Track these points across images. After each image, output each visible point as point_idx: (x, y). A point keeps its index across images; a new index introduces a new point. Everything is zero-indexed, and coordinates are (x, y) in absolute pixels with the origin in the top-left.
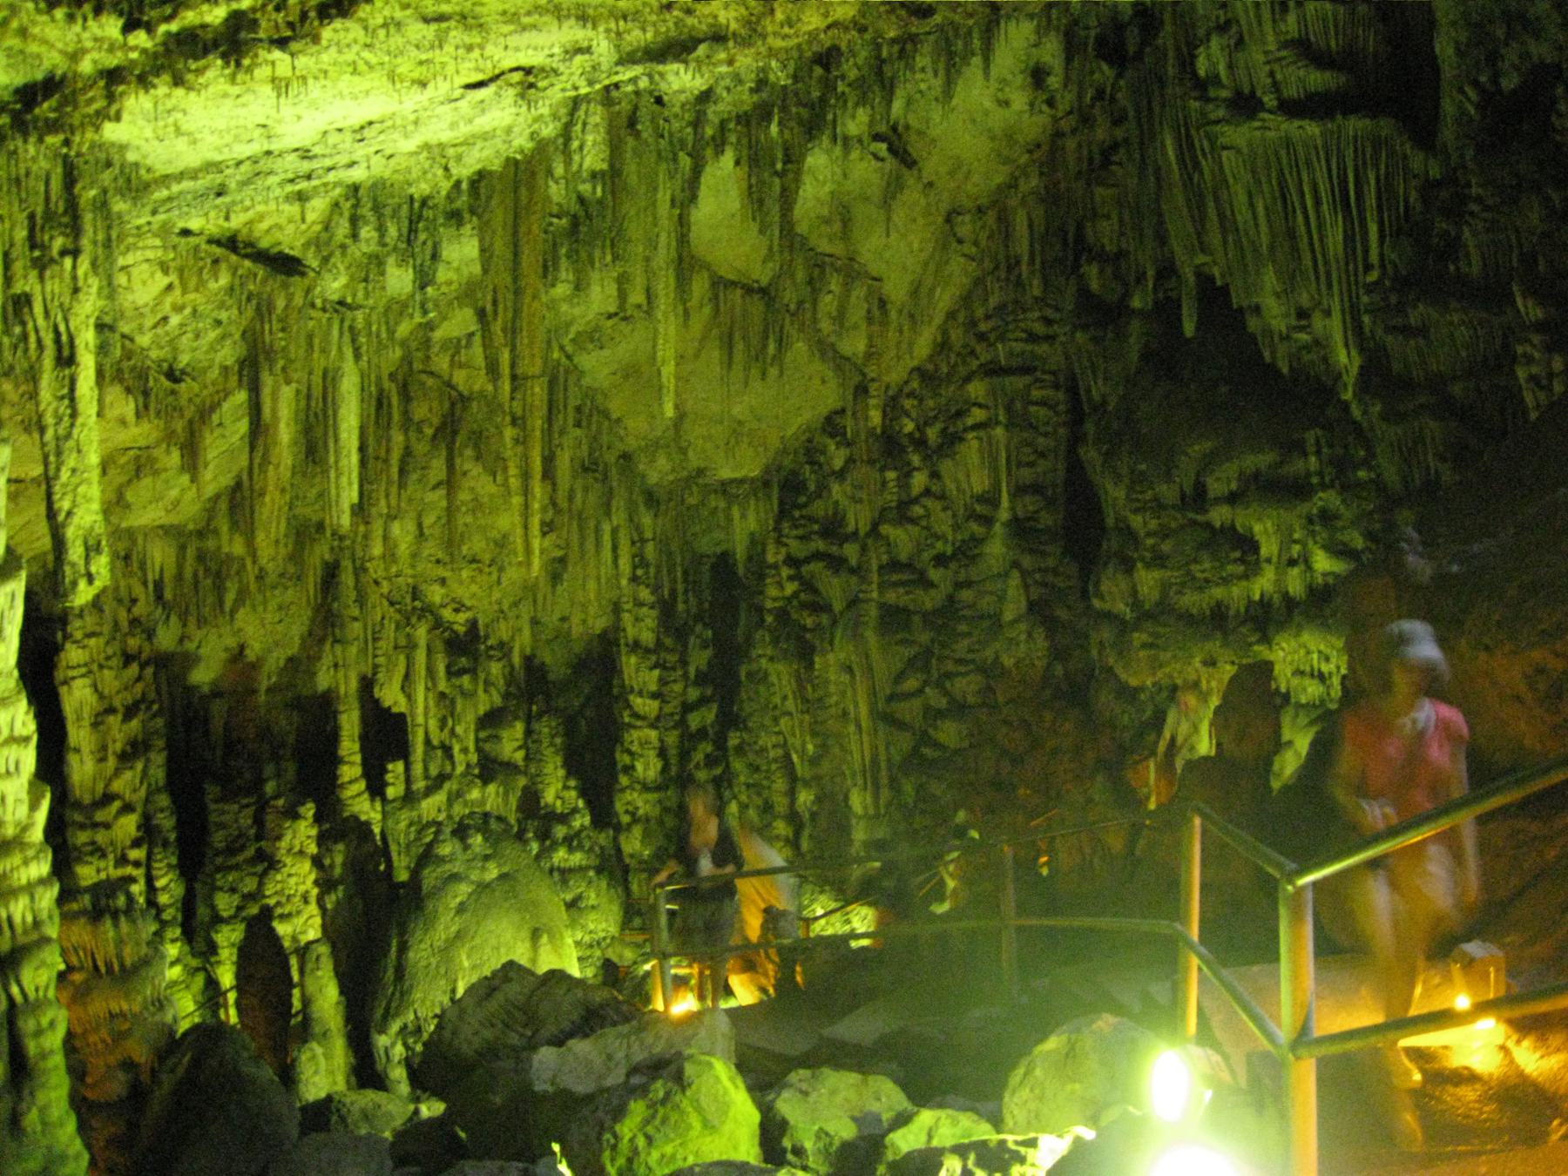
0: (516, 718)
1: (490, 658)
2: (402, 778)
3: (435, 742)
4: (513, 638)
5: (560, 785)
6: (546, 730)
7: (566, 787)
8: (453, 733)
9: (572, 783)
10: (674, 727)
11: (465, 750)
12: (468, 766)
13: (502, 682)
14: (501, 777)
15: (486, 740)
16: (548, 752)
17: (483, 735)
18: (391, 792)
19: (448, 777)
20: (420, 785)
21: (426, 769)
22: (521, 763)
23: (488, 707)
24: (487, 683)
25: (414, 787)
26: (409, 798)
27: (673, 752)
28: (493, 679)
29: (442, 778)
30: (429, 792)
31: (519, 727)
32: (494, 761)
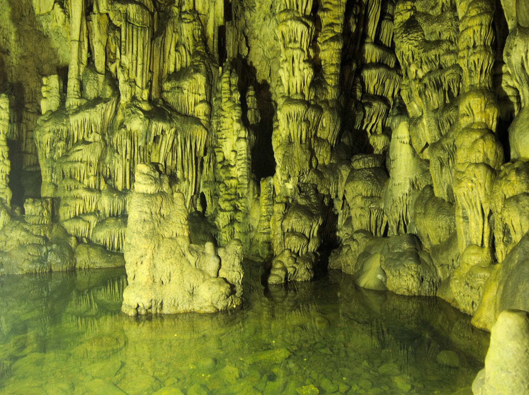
0: (197, 71)
1: (181, 20)
2: (55, 92)
3: (100, 66)
4: (209, 11)
5: (235, 138)
6: (226, 86)
7: (239, 139)
8: (120, 63)
9: (243, 134)
10: (332, 39)
11: (132, 83)
12: (134, 98)
13: (191, 40)
14: (177, 124)
15: (168, 92)
16: (226, 106)
17: (167, 86)
18: (45, 106)
19: (106, 101)
20: (72, 101)
21: (82, 89)
22: (202, 117)
23: (178, 67)
24: (177, 45)
25: (67, 104)
26: (61, 112)
27: (331, 71)
28: (184, 39)
29: (98, 100)
30: (80, 109)
31: (200, 79)
32: (179, 114)
